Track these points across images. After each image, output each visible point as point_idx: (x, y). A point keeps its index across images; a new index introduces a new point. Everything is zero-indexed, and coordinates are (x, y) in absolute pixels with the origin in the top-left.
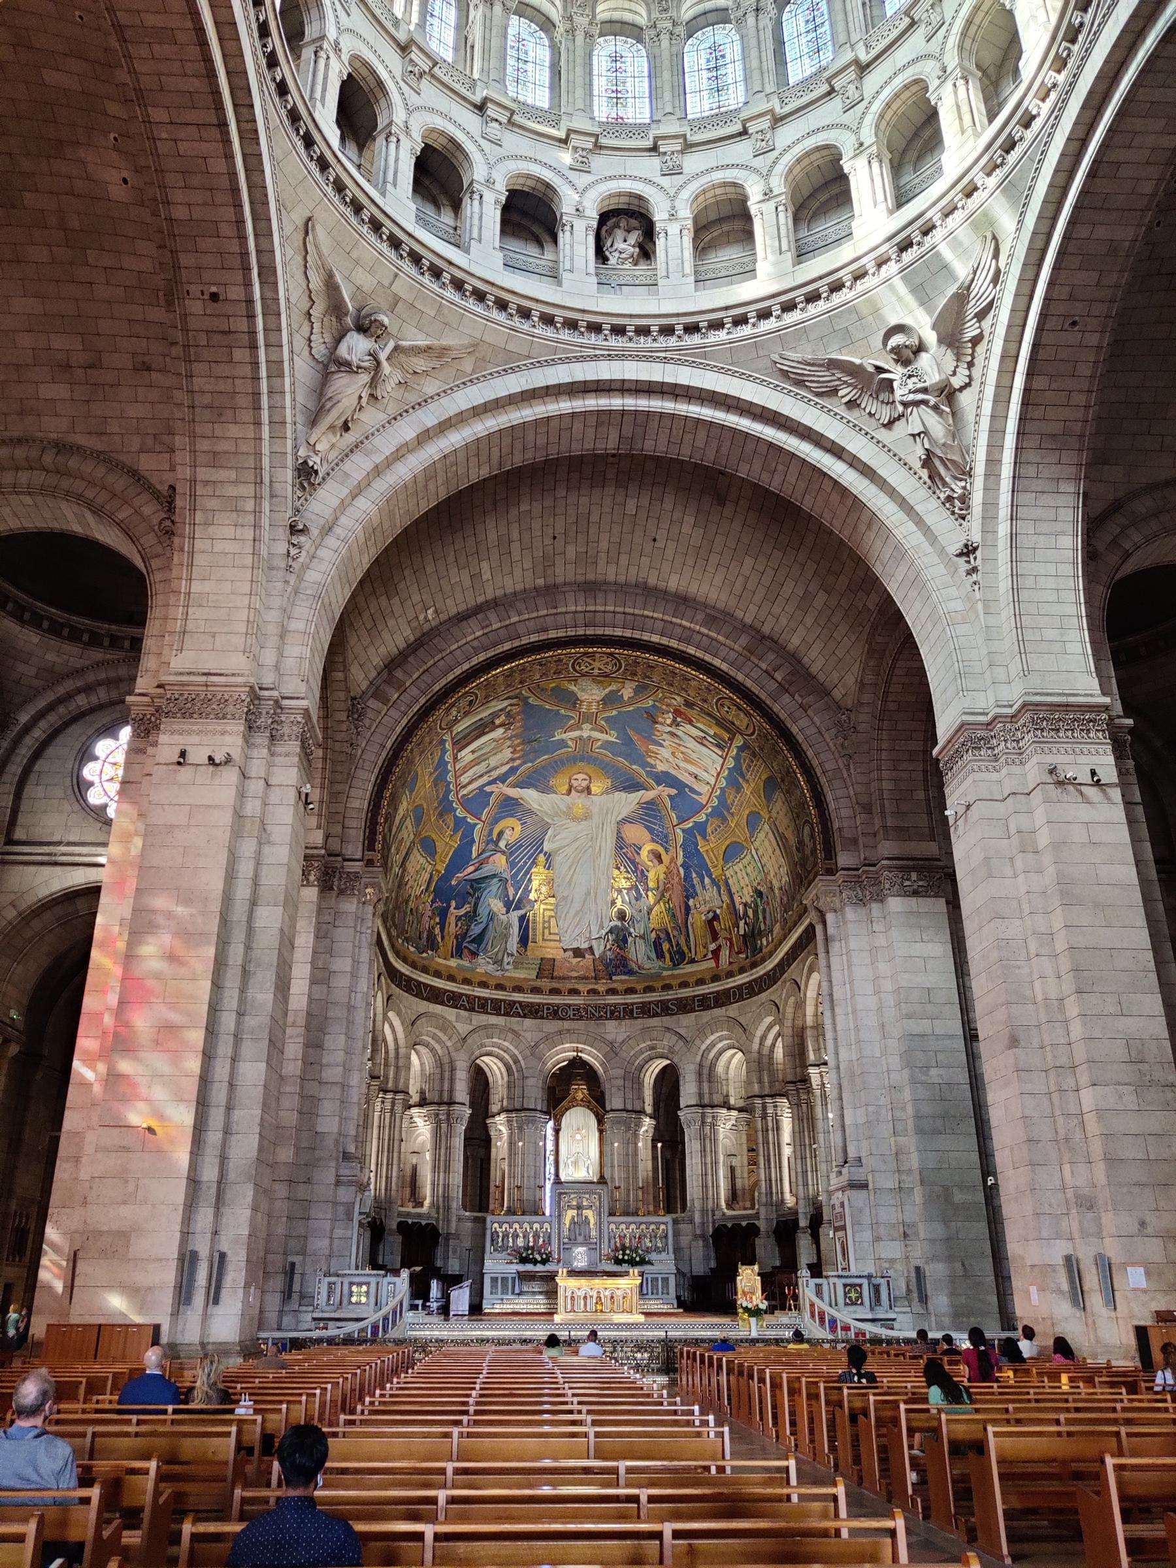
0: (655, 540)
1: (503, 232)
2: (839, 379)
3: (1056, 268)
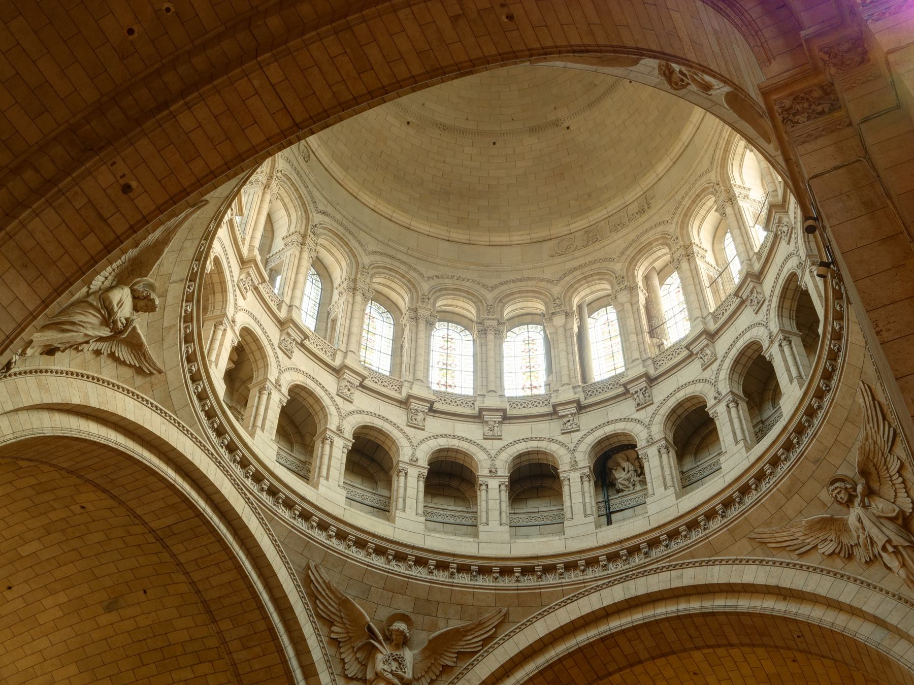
2: (341, 618)
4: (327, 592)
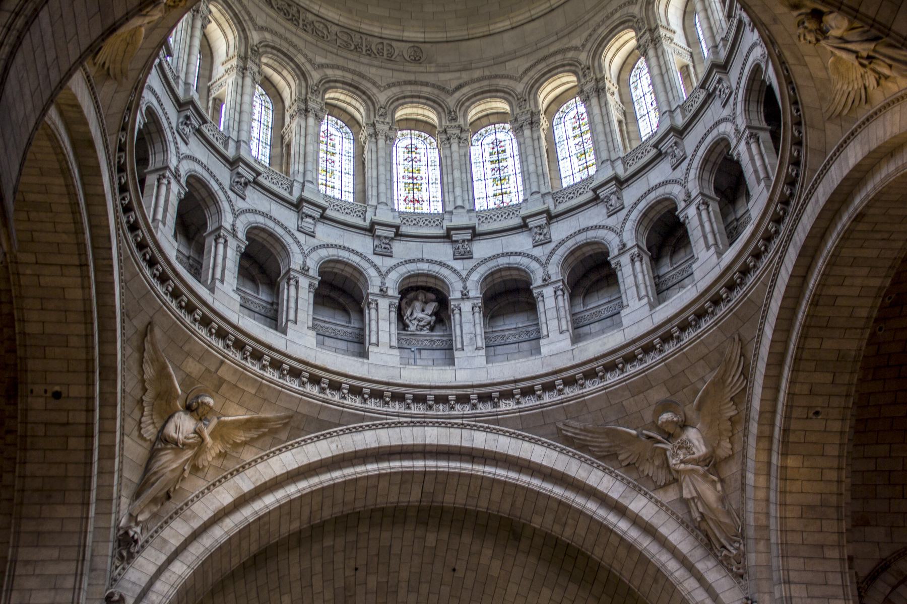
0: (454, 570)
1: (316, 303)
3: (795, 370)
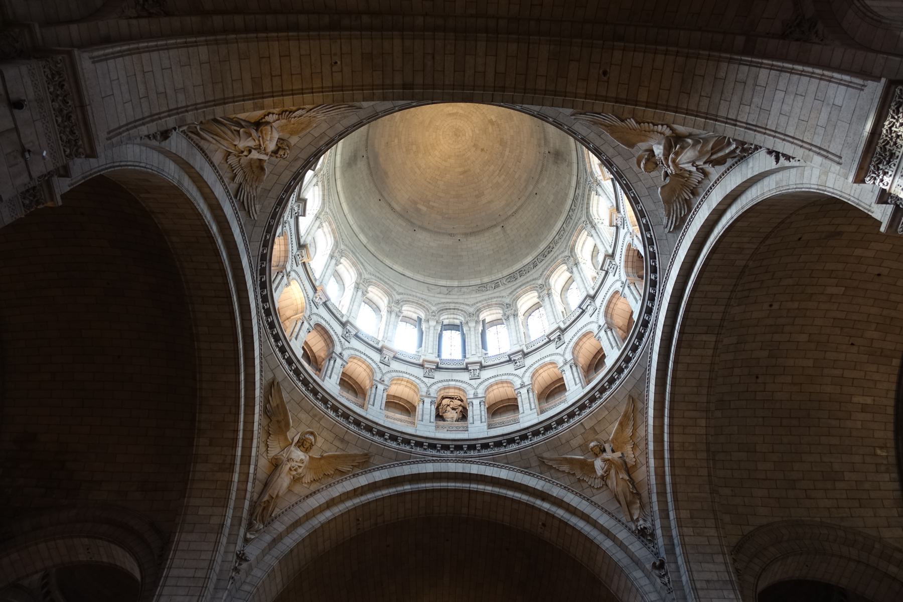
0: (879, 275)
2: (677, 198)
4: (672, 214)
